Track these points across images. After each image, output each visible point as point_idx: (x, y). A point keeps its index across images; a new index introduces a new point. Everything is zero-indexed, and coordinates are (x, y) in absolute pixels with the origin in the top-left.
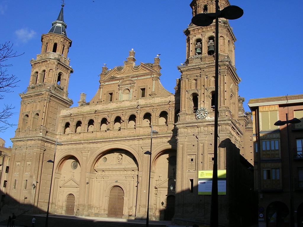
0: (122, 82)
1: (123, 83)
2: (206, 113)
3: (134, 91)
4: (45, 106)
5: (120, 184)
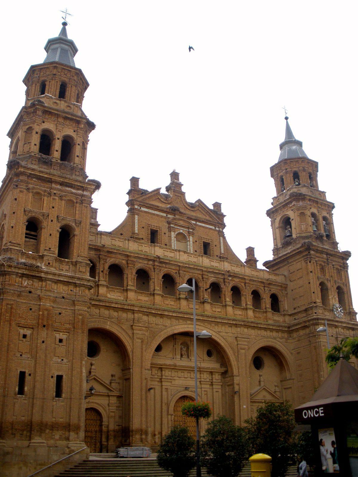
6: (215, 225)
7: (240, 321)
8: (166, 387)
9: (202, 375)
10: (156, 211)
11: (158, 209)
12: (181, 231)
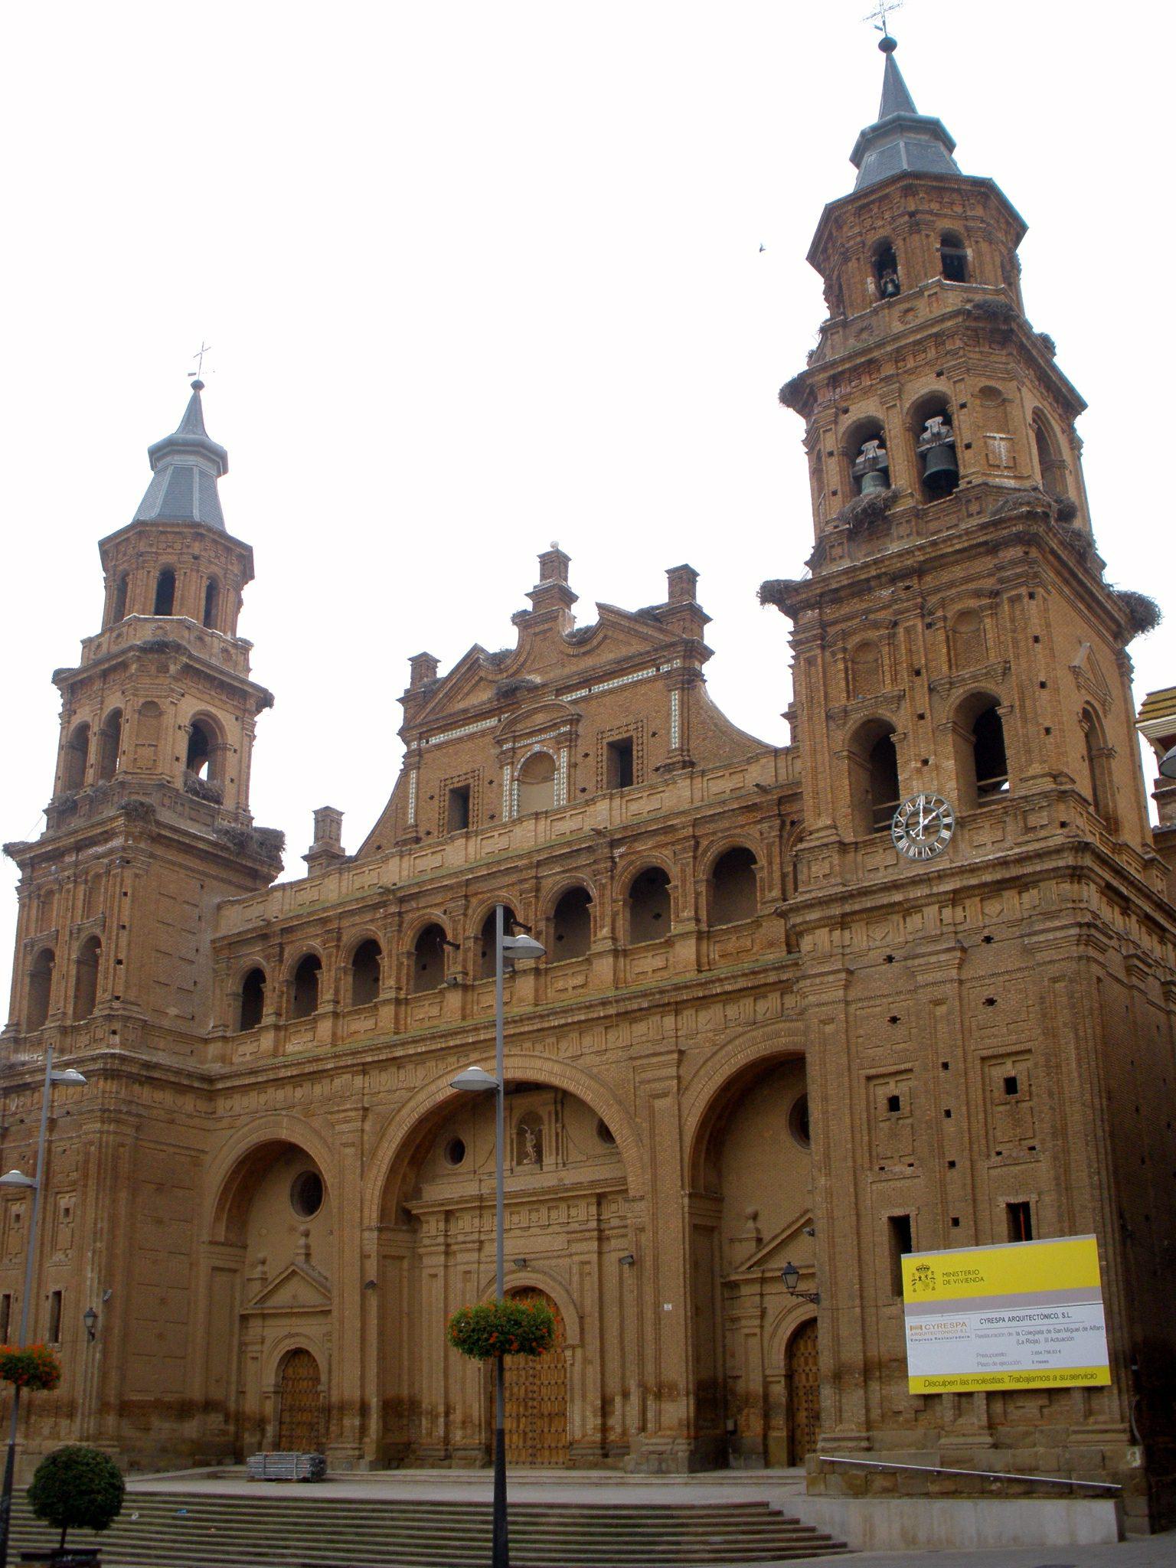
0: (513, 722)
1: (519, 726)
2: (947, 820)
3: (579, 759)
4: (125, 894)
5: (540, 1276)
6: (654, 660)
7: (629, 999)
8: (467, 1268)
9: (573, 1212)
10: (468, 724)
11: (469, 718)
12: (537, 748)
